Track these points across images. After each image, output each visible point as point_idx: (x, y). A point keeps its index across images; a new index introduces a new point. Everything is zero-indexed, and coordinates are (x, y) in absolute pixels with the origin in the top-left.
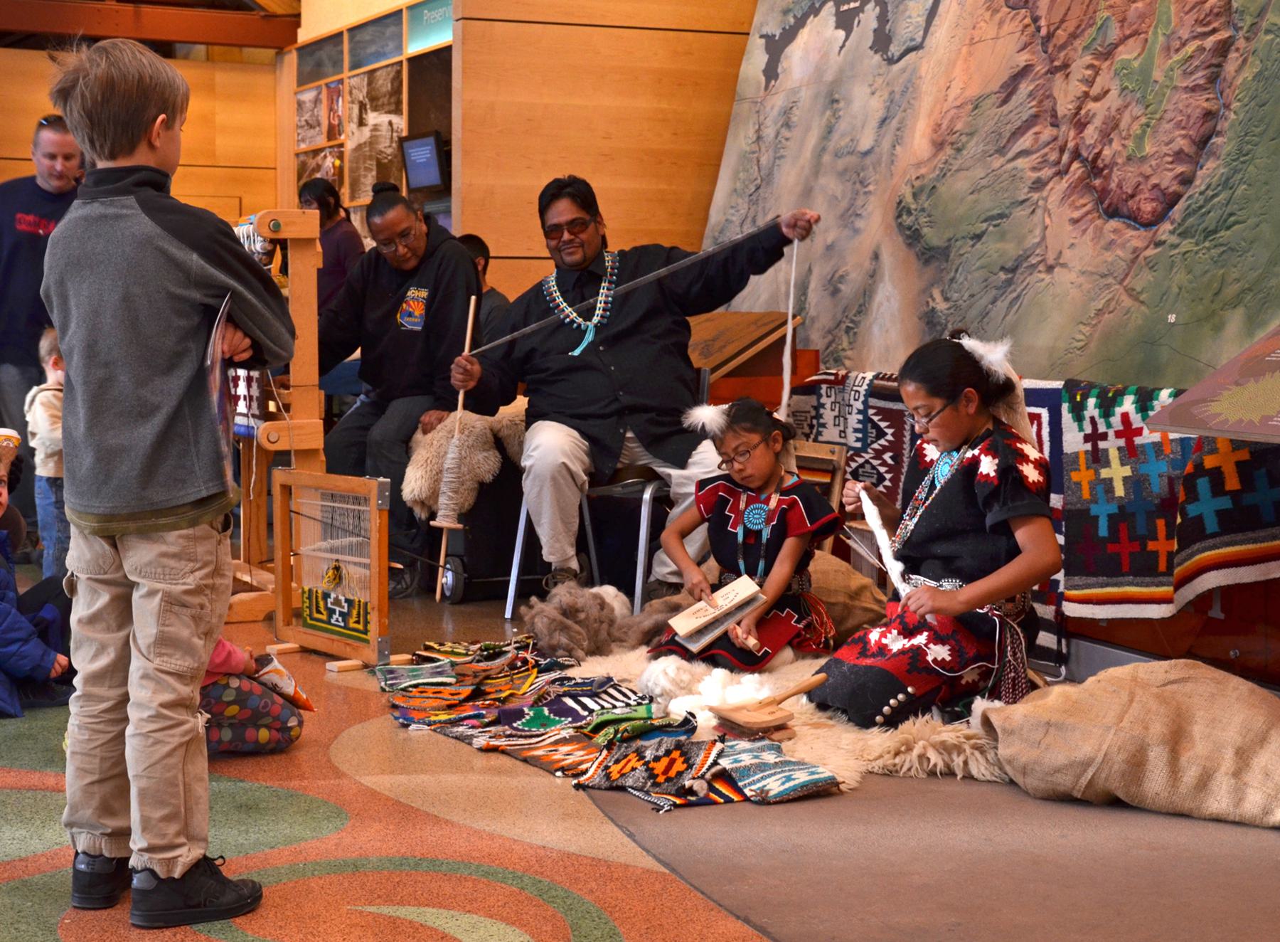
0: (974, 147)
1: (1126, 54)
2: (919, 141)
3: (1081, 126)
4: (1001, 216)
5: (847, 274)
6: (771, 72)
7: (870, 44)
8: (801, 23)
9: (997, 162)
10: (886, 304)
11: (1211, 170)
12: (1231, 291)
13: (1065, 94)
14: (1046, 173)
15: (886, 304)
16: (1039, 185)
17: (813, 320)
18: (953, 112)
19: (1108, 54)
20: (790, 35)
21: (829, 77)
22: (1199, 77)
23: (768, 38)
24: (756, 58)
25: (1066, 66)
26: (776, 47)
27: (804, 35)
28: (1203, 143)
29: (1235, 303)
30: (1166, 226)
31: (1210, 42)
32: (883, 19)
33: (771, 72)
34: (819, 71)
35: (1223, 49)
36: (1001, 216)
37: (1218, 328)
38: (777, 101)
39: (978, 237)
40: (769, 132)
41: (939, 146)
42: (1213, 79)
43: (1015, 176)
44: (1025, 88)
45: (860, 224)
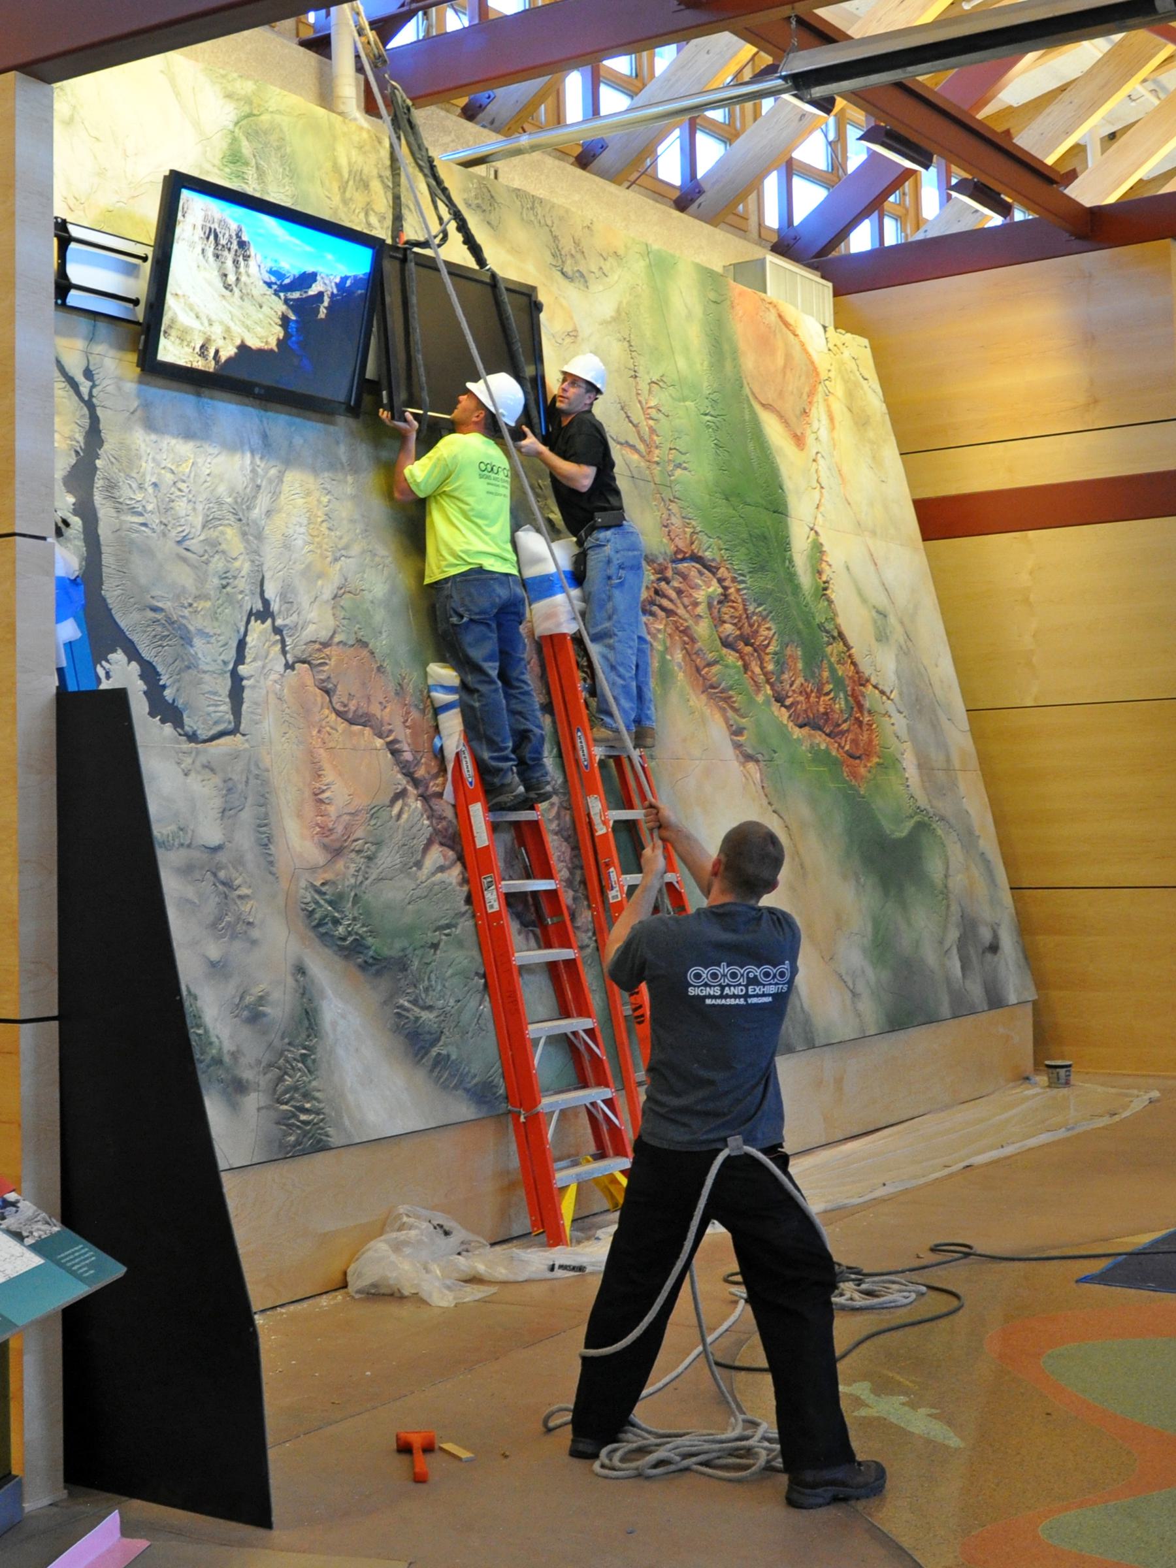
0: (388, 859)
2: (298, 842)
4: (448, 926)
5: (268, 994)
7: (147, 710)
10: (341, 1022)
15: (341, 1022)
17: (235, 1055)
18: (347, 818)
36: (448, 926)
39: (435, 946)
45: (255, 933)
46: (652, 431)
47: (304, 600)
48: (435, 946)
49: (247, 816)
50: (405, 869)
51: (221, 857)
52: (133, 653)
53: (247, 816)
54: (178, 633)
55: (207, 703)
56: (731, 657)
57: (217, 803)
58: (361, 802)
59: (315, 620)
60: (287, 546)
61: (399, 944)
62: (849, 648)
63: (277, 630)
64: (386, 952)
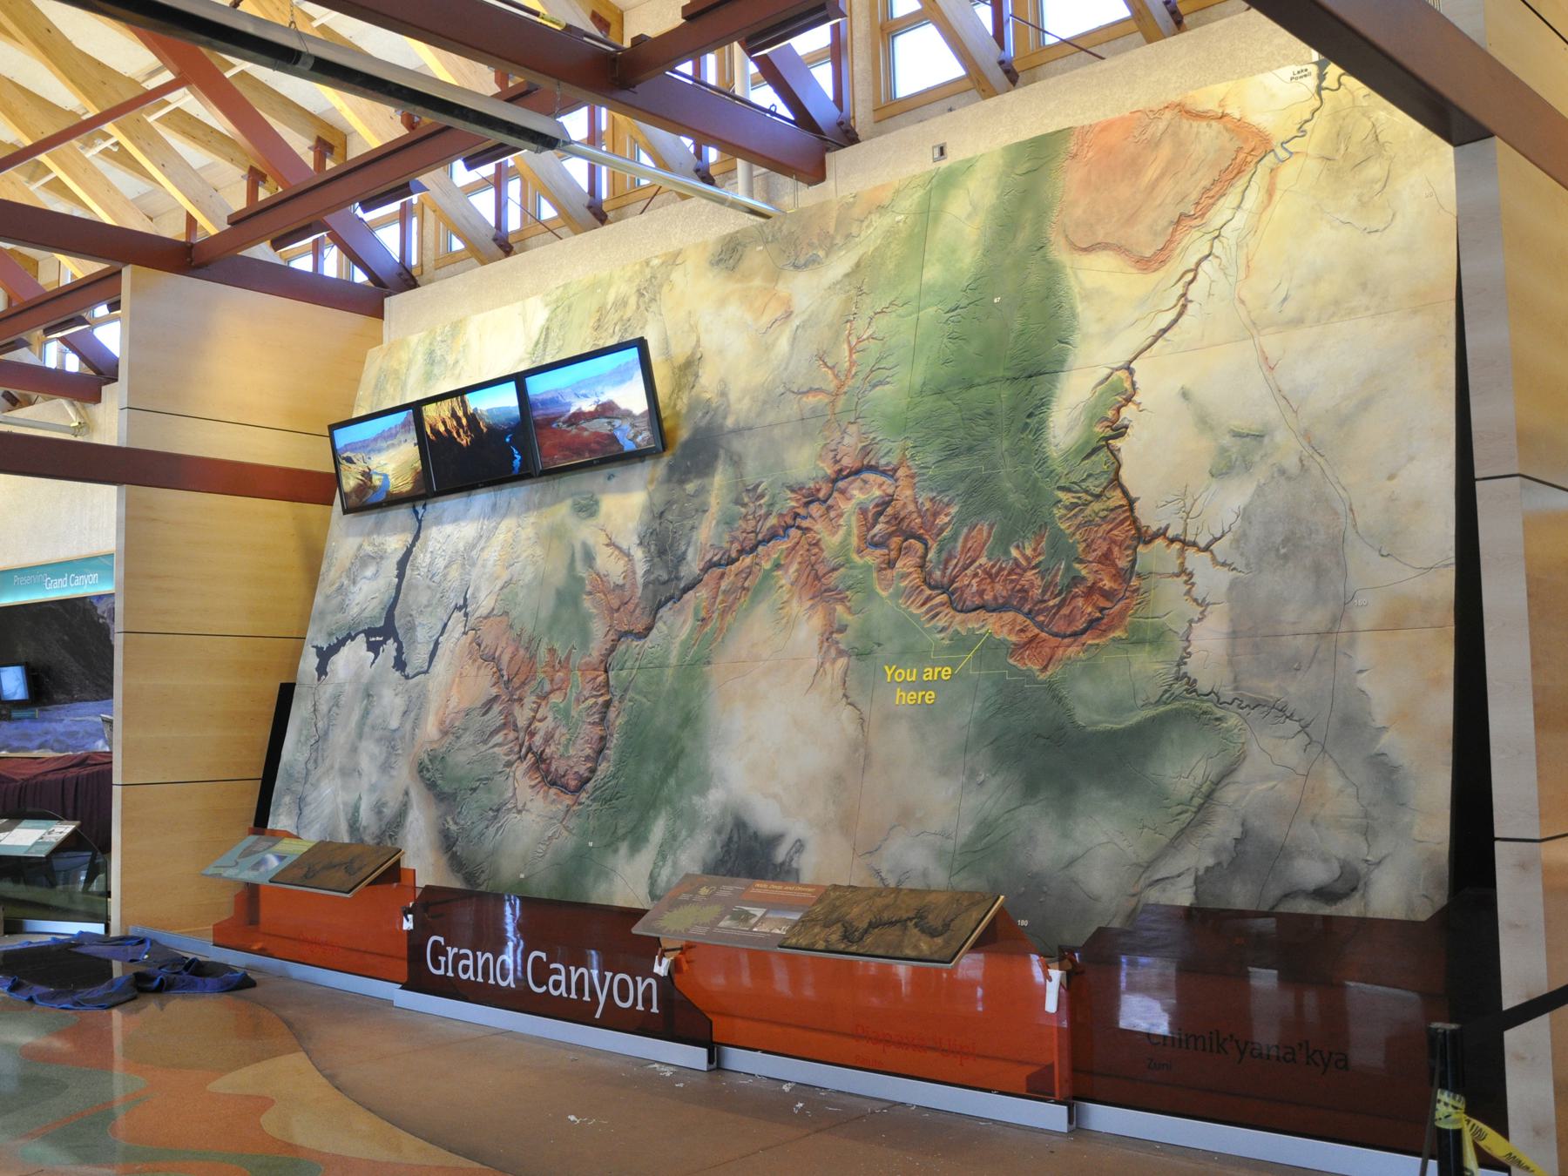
0: (467, 738)
1: (556, 698)
2: (430, 728)
3: (532, 734)
6: (322, 670)
8: (341, 643)
9: (483, 748)
11: (604, 768)
12: (621, 832)
13: (522, 716)
14: (513, 757)
16: (509, 764)
19: (545, 697)
20: (334, 649)
21: (365, 680)
22: (596, 718)
23: (319, 651)
24: (310, 661)
25: (520, 699)
26: (325, 655)
27: (344, 651)
28: (600, 751)
29: (623, 838)
30: (583, 796)
31: (601, 700)
32: (400, 650)
33: (322, 670)
34: (358, 675)
35: (607, 704)
37: (616, 851)
38: (327, 690)
39: (474, 790)
40: (323, 708)
41: (445, 733)
42: (603, 719)
43: (494, 757)
44: (497, 708)
45: (394, 773)
46: (852, 364)
47: (482, 595)
48: (474, 790)
49: (413, 715)
50: (474, 744)
51: (397, 735)
52: (397, 640)
53: (413, 715)
54: (411, 628)
55: (417, 658)
56: (873, 558)
57: (403, 709)
58: (465, 705)
59: (485, 602)
60: (484, 566)
61: (455, 786)
62: (1131, 502)
63: (466, 615)
64: (446, 789)
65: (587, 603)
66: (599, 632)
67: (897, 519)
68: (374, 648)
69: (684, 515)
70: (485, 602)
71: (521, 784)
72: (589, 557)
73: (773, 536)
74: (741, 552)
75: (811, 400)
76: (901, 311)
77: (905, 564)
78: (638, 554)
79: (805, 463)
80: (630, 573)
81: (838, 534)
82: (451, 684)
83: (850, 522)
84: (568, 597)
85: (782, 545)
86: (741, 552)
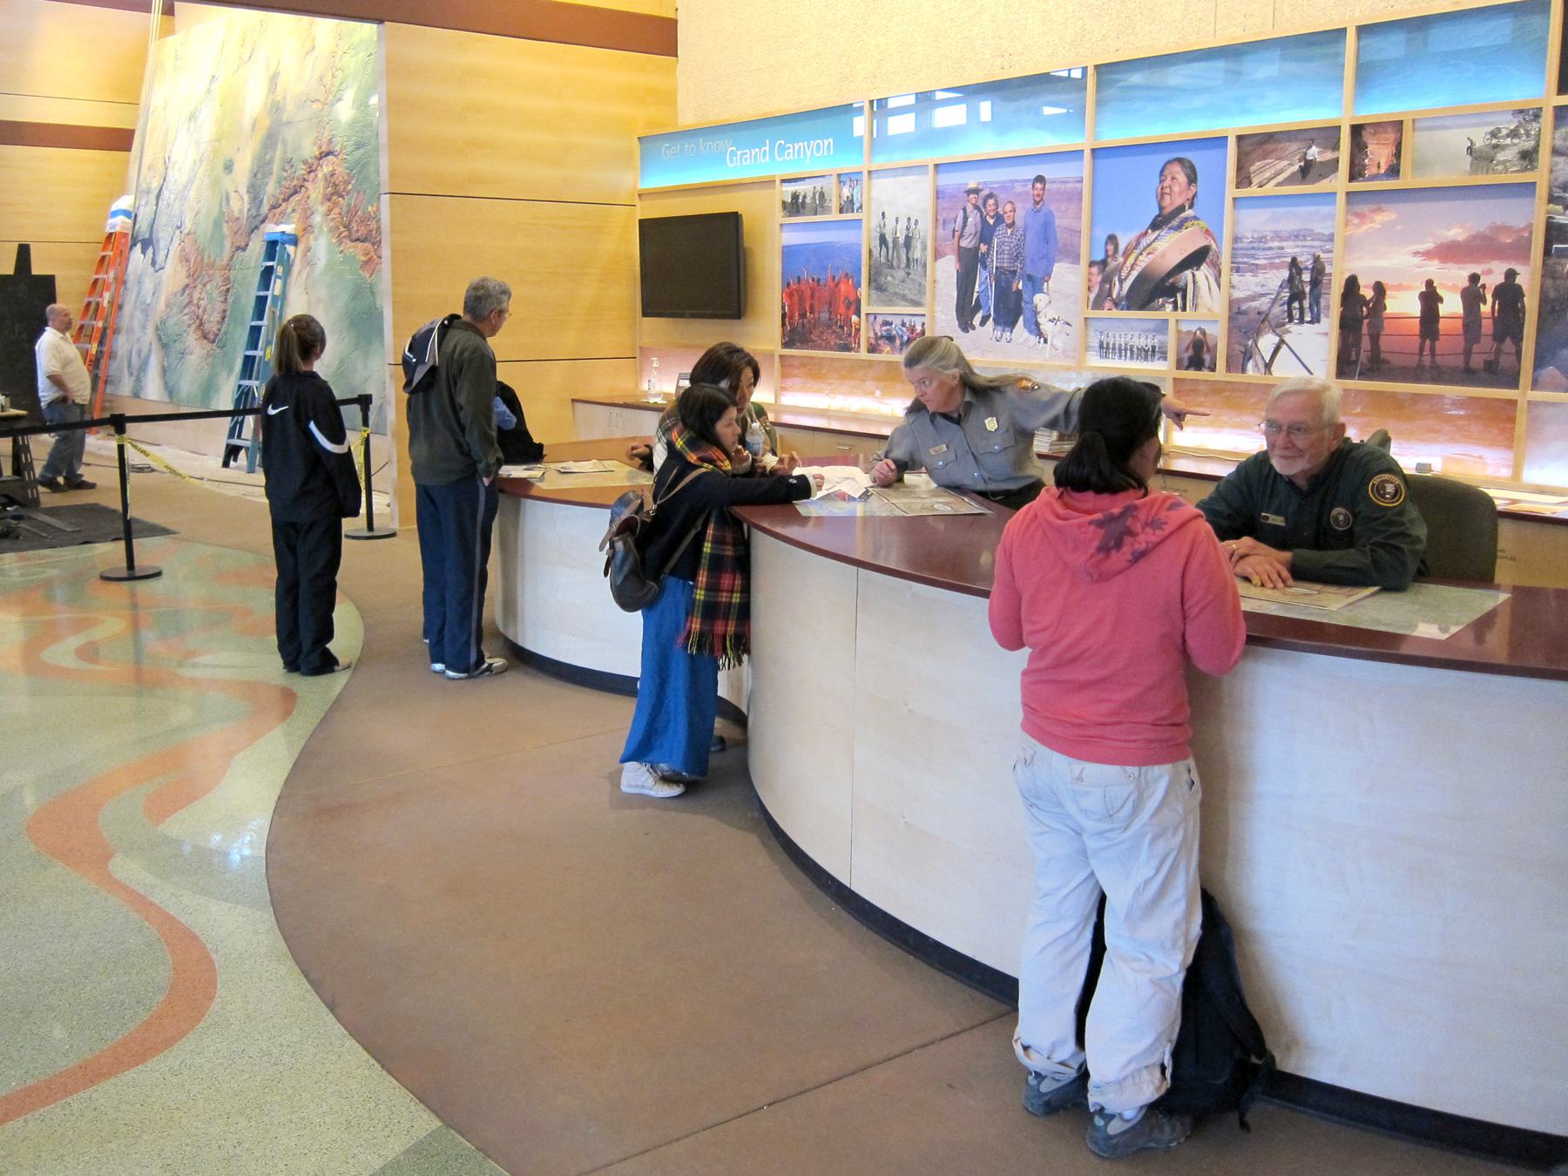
13: (196, 296)
65: (226, 230)
66: (227, 244)
67: (335, 185)
68: (144, 252)
69: (265, 176)
70: (188, 227)
71: (191, 339)
72: (228, 201)
73: (296, 192)
74: (284, 200)
75: (316, 106)
76: (352, 52)
77: (337, 210)
78: (246, 197)
79: (309, 150)
80: (241, 211)
81: (316, 191)
82: (173, 275)
83: (321, 184)
84: (217, 224)
85: (297, 197)
86: (284, 200)
